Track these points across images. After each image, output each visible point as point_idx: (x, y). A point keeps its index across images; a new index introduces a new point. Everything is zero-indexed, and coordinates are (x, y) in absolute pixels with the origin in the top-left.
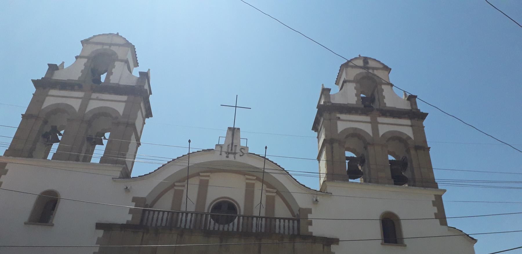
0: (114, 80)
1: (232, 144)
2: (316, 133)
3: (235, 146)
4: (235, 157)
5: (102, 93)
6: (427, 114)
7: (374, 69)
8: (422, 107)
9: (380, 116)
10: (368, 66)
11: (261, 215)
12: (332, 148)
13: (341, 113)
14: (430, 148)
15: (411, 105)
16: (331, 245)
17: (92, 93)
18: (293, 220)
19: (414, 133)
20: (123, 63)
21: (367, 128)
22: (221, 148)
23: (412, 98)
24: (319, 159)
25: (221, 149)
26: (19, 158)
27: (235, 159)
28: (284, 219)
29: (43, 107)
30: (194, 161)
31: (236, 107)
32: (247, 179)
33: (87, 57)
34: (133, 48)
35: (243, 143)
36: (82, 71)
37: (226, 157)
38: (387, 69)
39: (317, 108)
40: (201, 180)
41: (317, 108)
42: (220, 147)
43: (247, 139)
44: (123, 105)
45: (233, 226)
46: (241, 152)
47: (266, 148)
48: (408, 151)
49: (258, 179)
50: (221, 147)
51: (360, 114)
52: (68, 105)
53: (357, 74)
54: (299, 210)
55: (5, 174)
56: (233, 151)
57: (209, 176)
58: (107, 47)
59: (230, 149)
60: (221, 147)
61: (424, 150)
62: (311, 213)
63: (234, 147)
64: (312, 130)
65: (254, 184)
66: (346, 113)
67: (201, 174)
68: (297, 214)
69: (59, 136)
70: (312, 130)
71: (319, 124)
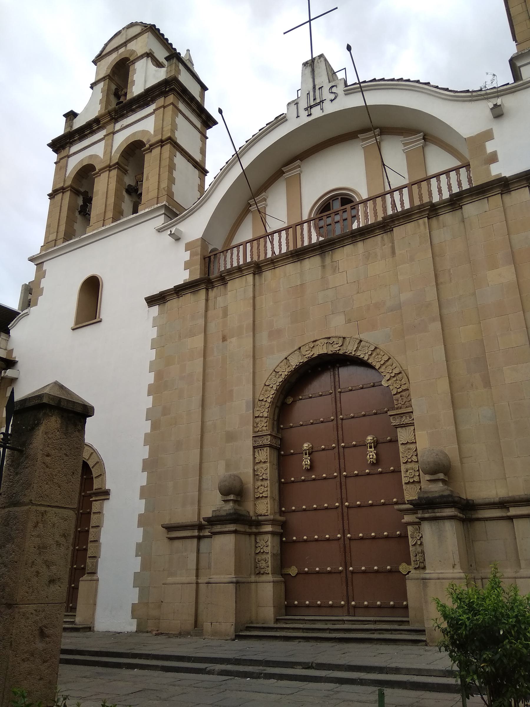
3: (319, 88)
25: (297, 109)
27: (323, 112)
29: (67, 176)
33: (103, 79)
34: (153, 30)
37: (307, 116)
42: (295, 104)
43: (345, 69)
46: (332, 93)
47: (349, 48)
52: (91, 156)
56: (318, 101)
59: (312, 99)
60: (297, 104)
63: (317, 91)
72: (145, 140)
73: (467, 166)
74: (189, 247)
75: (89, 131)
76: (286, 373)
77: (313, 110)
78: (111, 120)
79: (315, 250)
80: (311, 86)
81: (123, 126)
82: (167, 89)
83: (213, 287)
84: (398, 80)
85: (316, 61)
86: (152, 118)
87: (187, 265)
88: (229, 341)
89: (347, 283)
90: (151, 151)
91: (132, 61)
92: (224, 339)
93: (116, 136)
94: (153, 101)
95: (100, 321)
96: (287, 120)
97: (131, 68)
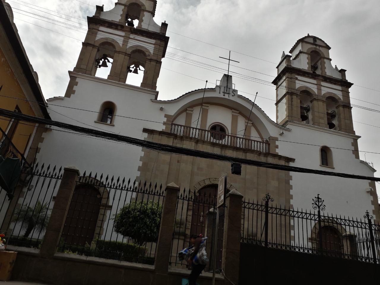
0: (145, 26)
1: (227, 86)
2: (275, 86)
6: (353, 84)
7: (320, 46)
8: (349, 78)
9: (323, 81)
10: (316, 43)
12: (292, 98)
13: (299, 75)
14: (352, 107)
15: (342, 76)
18: (266, 144)
19: (343, 96)
20: (150, 14)
21: (314, 89)
23: (343, 71)
24: (277, 104)
26: (85, 75)
28: (260, 142)
30: (208, 95)
31: (229, 60)
33: (125, 5)
35: (233, 88)
36: (121, 15)
38: (329, 48)
39: (277, 67)
45: (225, 141)
46: (233, 93)
47: (257, 93)
48: (337, 107)
49: (240, 113)
50: (220, 88)
51: (310, 78)
52: (113, 40)
53: (309, 48)
55: (76, 85)
57: (208, 107)
59: (226, 90)
60: (220, 88)
61: (349, 108)
63: (228, 89)
66: (301, 75)
68: (267, 140)
69: (108, 62)
72: (147, 53)
73: (269, 144)
74: (166, 116)
75: (115, 27)
76: (203, 185)
77: (226, 94)
79: (219, 146)
80: (226, 86)
81: (134, 38)
83: (176, 139)
85: (229, 77)
86: (153, 46)
87: (164, 123)
88: (181, 164)
90: (151, 62)
91: (143, 10)
92: (178, 162)
93: (130, 41)
94: (154, 38)
95: (114, 126)
96: (215, 91)
97: (142, 12)
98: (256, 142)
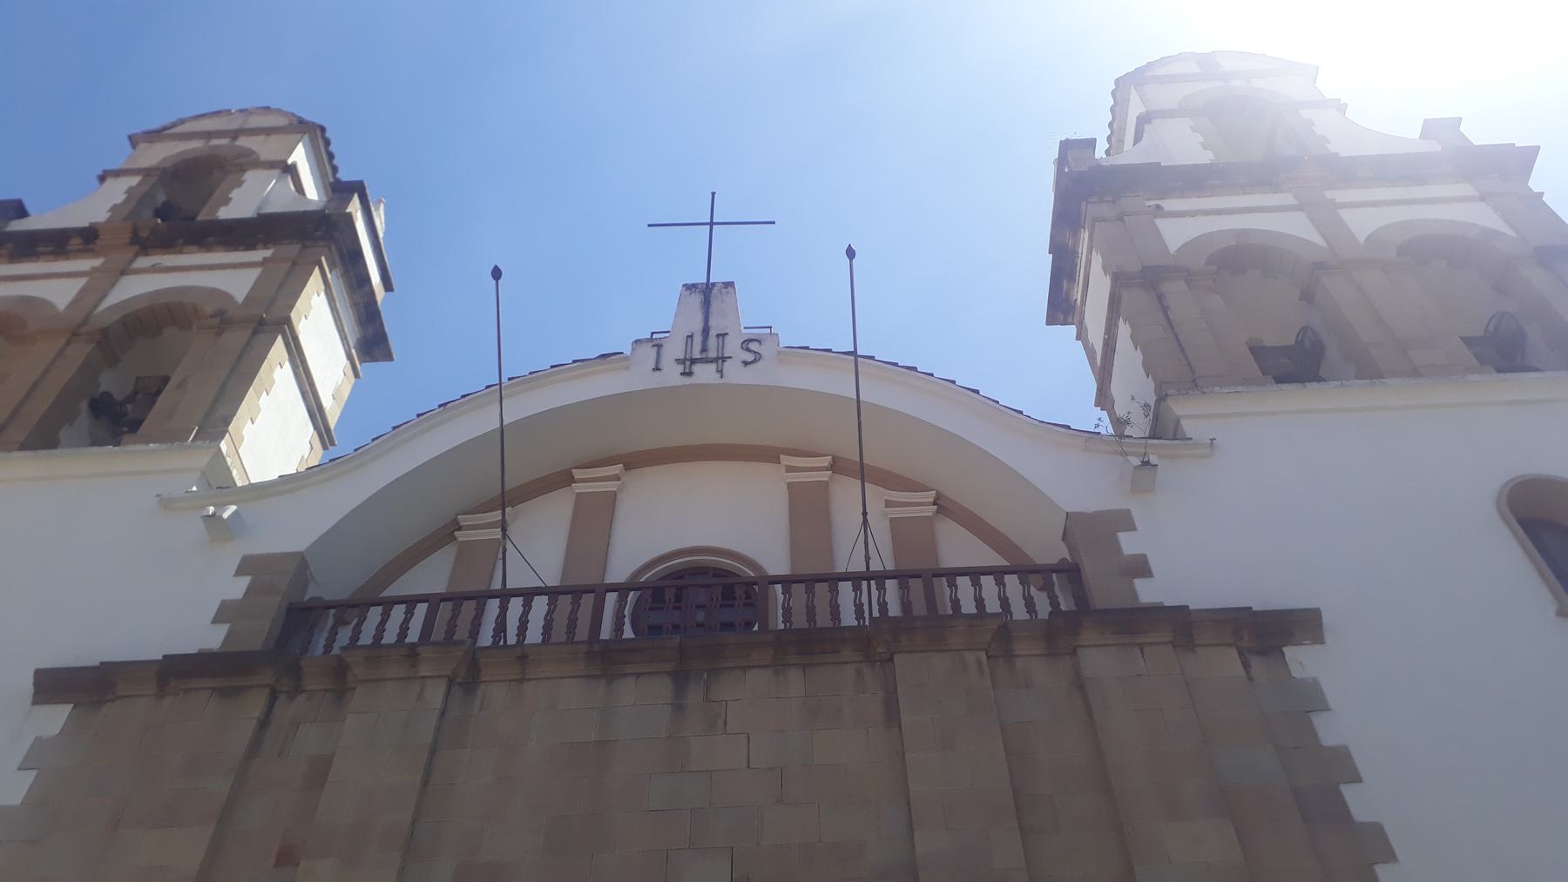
1: (706, 331)
3: (722, 336)
4: (720, 372)
5: (175, 253)
11: (875, 566)
16: (1285, 649)
17: (137, 255)
20: (276, 172)
22: (655, 349)
25: (658, 354)
27: (722, 377)
28: (998, 573)
31: (711, 224)
32: (790, 469)
33: (146, 172)
37: (682, 374)
40: (579, 495)
41: (1050, 253)
42: (654, 346)
44: (254, 274)
46: (748, 350)
47: (851, 253)
54: (1064, 538)
56: (712, 354)
58: (224, 142)
62: (1130, 526)
63: (712, 342)
64: (1051, 320)
65: (824, 486)
67: (578, 474)
70: (1051, 320)
71: (1072, 278)
74: (247, 566)
75: (50, 249)
77: (697, 368)
78: (132, 243)
80: (697, 326)
82: (318, 233)
83: (298, 690)
84: (908, 368)
85: (715, 290)
87: (225, 612)
89: (749, 767)
90: (219, 334)
96: (627, 368)
98: (964, 583)
